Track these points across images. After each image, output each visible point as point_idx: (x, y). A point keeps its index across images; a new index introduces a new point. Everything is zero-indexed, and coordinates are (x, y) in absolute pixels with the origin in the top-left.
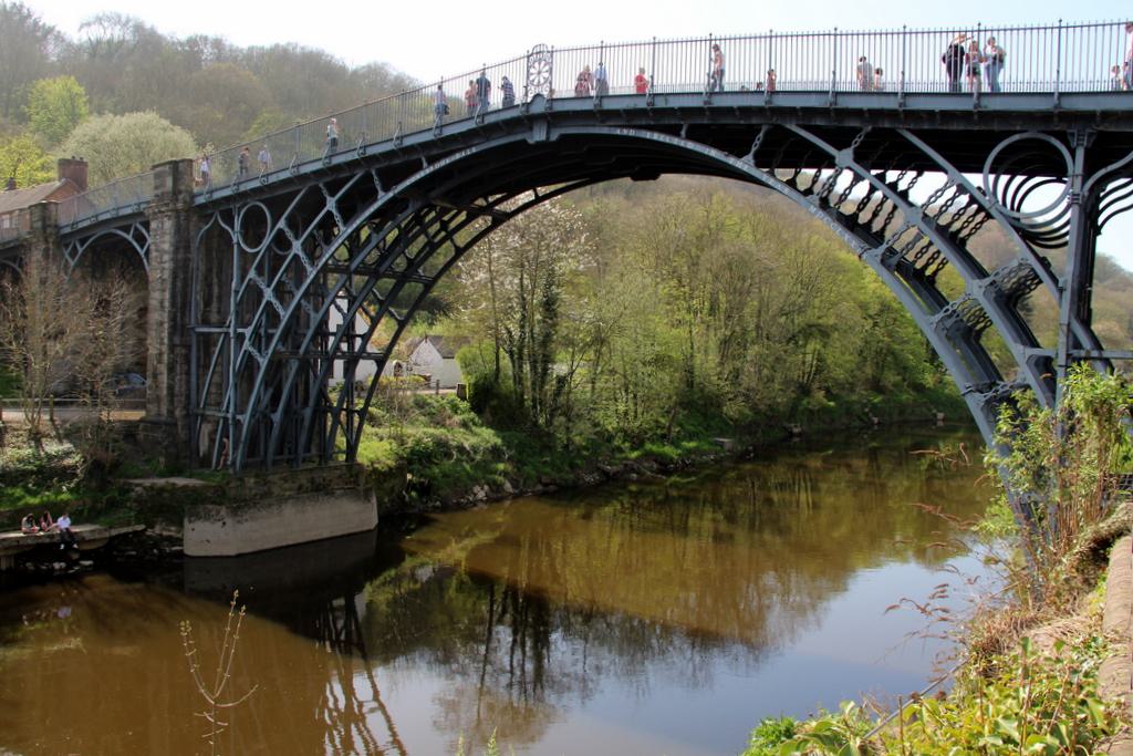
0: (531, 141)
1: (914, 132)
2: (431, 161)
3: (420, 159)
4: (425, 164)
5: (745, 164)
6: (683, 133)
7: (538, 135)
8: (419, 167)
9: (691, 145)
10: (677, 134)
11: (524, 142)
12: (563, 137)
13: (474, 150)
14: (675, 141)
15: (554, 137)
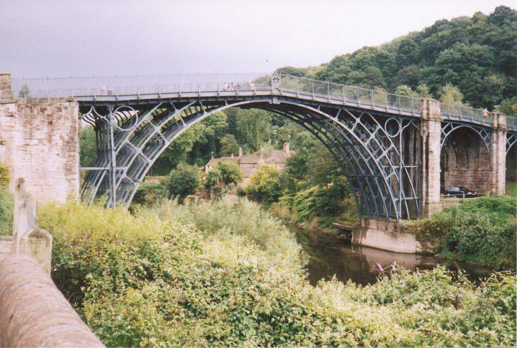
0: (271, 103)
1: (373, 116)
2: (229, 103)
3: (224, 101)
4: (227, 104)
5: (336, 119)
6: (319, 109)
7: (276, 101)
8: (224, 105)
9: (321, 113)
10: (317, 108)
11: (268, 103)
12: (281, 104)
13: (248, 102)
14: (318, 111)
15: (279, 103)
